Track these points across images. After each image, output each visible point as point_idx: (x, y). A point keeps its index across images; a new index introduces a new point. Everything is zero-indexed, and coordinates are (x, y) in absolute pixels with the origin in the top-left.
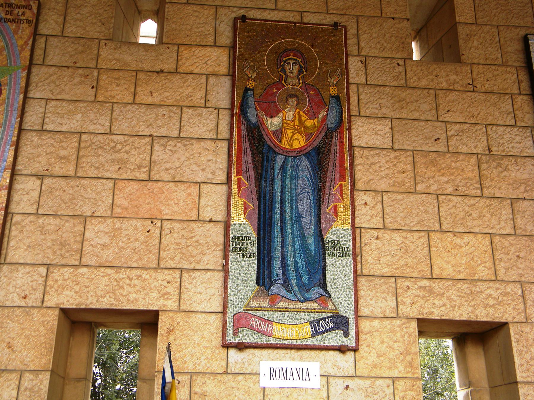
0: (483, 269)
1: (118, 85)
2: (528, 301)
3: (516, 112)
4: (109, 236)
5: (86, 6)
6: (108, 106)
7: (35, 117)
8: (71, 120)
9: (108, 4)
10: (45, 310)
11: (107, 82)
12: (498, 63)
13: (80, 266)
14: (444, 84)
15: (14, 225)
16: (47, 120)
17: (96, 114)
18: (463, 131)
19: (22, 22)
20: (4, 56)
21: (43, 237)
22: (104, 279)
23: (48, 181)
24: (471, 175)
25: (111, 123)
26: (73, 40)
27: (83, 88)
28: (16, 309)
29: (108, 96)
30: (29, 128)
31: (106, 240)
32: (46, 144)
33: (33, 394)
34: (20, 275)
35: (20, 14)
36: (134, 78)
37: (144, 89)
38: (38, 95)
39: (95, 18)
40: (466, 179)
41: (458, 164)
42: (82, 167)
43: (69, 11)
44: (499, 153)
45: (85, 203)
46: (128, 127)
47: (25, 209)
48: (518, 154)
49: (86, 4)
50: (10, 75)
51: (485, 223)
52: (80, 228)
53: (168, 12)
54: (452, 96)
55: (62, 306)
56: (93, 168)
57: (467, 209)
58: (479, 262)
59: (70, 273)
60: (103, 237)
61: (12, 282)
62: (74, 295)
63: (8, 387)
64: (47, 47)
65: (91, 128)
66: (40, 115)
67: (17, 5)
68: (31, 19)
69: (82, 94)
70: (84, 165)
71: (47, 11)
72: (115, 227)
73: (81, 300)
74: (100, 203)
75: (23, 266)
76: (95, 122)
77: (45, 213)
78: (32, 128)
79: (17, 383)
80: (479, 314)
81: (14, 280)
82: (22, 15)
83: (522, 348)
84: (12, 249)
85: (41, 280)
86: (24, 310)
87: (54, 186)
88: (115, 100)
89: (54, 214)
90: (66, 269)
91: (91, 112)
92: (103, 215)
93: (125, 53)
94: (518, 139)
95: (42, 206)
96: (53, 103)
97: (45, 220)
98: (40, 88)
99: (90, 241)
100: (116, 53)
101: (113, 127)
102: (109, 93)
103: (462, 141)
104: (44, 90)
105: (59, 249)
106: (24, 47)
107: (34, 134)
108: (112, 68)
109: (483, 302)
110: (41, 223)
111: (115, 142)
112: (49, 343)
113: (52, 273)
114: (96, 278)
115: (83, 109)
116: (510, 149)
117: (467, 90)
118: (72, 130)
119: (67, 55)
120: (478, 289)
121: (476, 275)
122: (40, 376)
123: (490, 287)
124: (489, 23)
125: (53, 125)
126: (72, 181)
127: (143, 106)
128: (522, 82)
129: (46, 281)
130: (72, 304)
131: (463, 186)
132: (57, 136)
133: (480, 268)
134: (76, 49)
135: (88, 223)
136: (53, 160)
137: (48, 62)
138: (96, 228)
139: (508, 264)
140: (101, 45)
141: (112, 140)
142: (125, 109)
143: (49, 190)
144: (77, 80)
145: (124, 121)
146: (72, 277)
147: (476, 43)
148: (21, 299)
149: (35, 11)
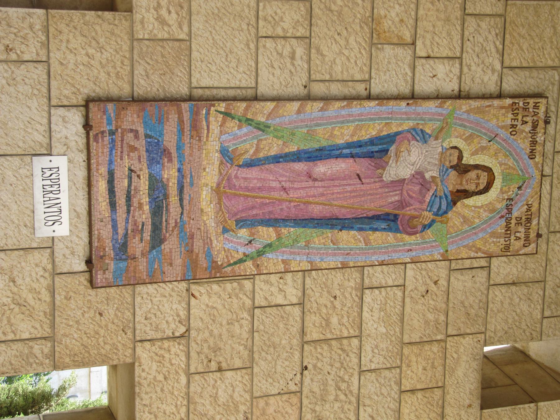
1: (425, 369)
4: (228, 401)
5: (529, 306)
6: (396, 362)
7: (381, 276)
8: (377, 320)
9: (533, 333)
10: (132, 346)
11: (429, 353)
13: (189, 375)
15: (238, 283)
16: (377, 291)
17: (385, 350)
19: (507, 239)
20: (460, 228)
21: (224, 322)
22: (173, 407)
23: (297, 311)
25: (374, 370)
26: (484, 300)
27: (420, 327)
28: (132, 311)
29: (409, 358)
30: (366, 272)
31: (223, 397)
32: (346, 298)
33: (25, 358)
34: (174, 307)
35: (518, 235)
36: (434, 386)
37: (419, 401)
38: (410, 273)
39: (515, 321)
42: (315, 348)
43: (523, 287)
45: (270, 362)
46: (370, 392)
47: (260, 292)
49: (532, 306)
50: (435, 241)
52: (238, 363)
53: (524, 409)
55: (137, 364)
56: (315, 362)
59: (179, 364)
60: (226, 394)
61: (166, 299)
62: (151, 377)
63: (33, 327)
64: (473, 270)
65: (367, 347)
66: (384, 282)
67: (529, 229)
68: (511, 249)
69: (412, 327)
70: (319, 350)
71: (523, 261)
72: (239, 405)
73: (146, 386)
74: (270, 380)
75: (186, 306)
76: (376, 351)
77: (255, 317)
78: (366, 275)
79: (39, 336)
81: (168, 301)
82: (517, 237)
84: (208, 289)
85: (169, 333)
86: (130, 320)
87: (291, 319)
88: (404, 368)
89: (255, 328)
90: (184, 359)
91: (389, 342)
92: (255, 387)
93: (467, 367)
95: (265, 312)
96: (400, 294)
97: (247, 320)
98: (419, 274)
99: (221, 379)
100: (468, 355)
101: (370, 374)
102: (414, 359)
104: (416, 279)
105: (209, 346)
106: (474, 249)
107: (358, 280)
108: (448, 356)
110: (242, 316)
111: (350, 379)
112: (89, 360)
113: (179, 344)
114: (174, 397)
115: (392, 333)
118: (364, 325)
119: (464, 297)
122: (48, 360)
125: (370, 301)
126: (297, 340)
127: (397, 405)
129: (168, 338)
130: (140, 377)
132: (356, 309)
134: (471, 306)
135: (244, 371)
136: (324, 310)
137: (454, 275)
138: (237, 383)
140: (478, 335)
141: (352, 375)
142: (393, 383)
143: (285, 315)
144: (430, 317)
145: (378, 385)
146: (174, 368)
148: (144, 315)
149: (521, 252)
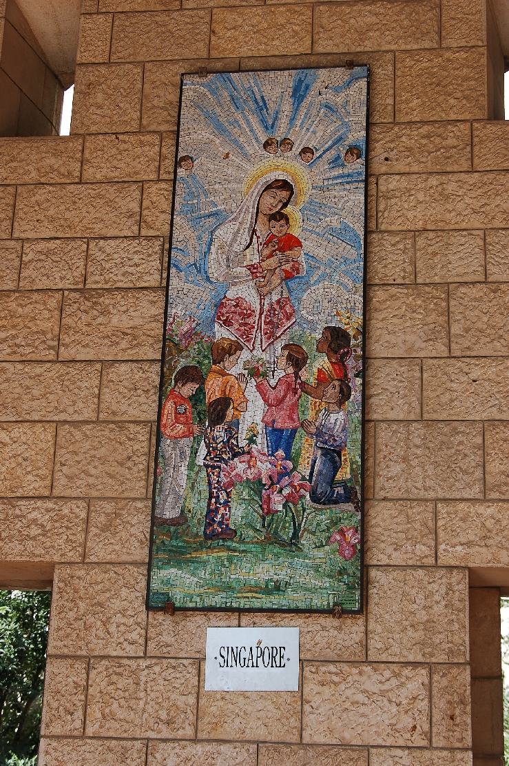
0: (33, 479)
2: (92, 529)
3: (145, 213)
12: (132, 129)
14: (34, 174)
18: (48, 253)
24: (46, 325)
40: (37, 332)
41: (28, 309)
44: (99, 286)
48: (131, 285)
51: (52, 404)
54: (41, 195)
57: (28, 382)
58: (29, 469)
80: (9, 551)
83: (66, 603)
94: (136, 259)
103: (42, 270)
109: (20, 532)
116: (120, 278)
117: (68, 181)
120: (18, 512)
121: (20, 490)
123: (38, 508)
124: (131, 59)
128: (166, 158)
131: (28, 345)
133: (30, 477)
139: (75, 470)
147: (100, 97)
